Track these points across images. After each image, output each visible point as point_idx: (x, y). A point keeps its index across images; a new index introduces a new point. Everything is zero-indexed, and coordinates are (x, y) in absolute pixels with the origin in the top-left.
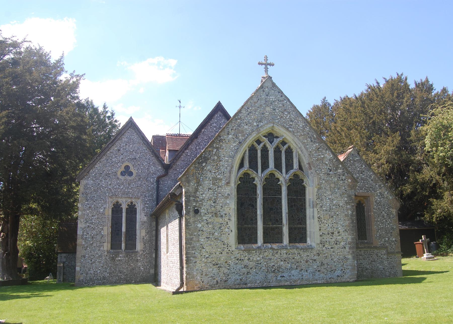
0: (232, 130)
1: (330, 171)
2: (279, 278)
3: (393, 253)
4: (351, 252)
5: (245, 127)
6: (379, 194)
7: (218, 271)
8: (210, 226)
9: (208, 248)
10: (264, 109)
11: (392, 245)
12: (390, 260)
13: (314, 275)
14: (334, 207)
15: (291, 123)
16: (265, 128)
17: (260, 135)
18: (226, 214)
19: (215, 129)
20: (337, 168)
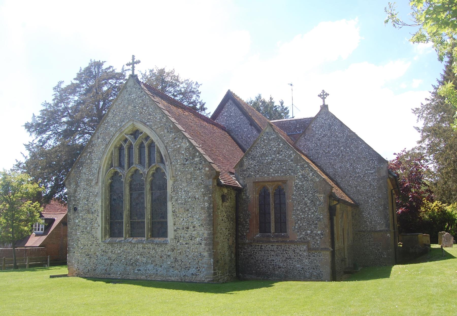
1: (186, 161)
3: (316, 249)
4: (207, 249)
5: (111, 129)
6: (300, 177)
7: (89, 261)
8: (84, 222)
9: (82, 240)
11: (317, 240)
12: (312, 258)
13: (168, 271)
15: (149, 117)
16: (126, 127)
17: (123, 134)
20: (194, 157)
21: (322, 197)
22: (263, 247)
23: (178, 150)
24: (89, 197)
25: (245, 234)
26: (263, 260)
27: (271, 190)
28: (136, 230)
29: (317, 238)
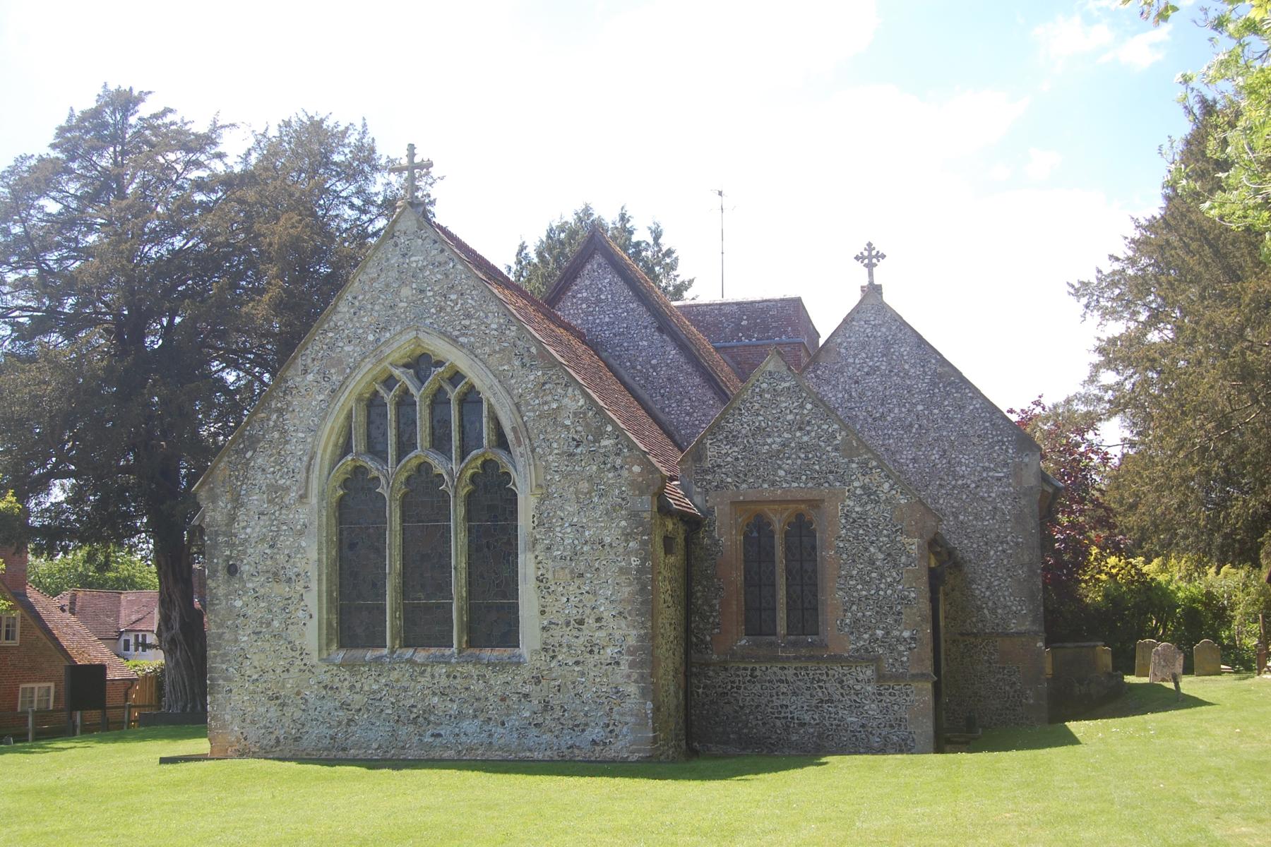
0: (313, 360)
1: (577, 446)
2: (428, 739)
3: (897, 678)
4: (635, 676)
6: (859, 492)
7: (280, 713)
8: (262, 605)
9: (256, 658)
10: (397, 293)
11: (901, 654)
12: (887, 698)
14: (585, 549)
15: (467, 322)
16: (395, 345)
17: (386, 364)
18: (298, 575)
19: (584, 306)
20: (599, 435)
21: (914, 545)
22: (758, 673)
23: (554, 416)
24: (278, 535)
25: (708, 638)
26: (757, 707)
27: (778, 525)
28: (423, 628)
29: (902, 648)
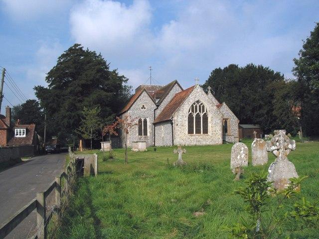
28: (198, 132)
